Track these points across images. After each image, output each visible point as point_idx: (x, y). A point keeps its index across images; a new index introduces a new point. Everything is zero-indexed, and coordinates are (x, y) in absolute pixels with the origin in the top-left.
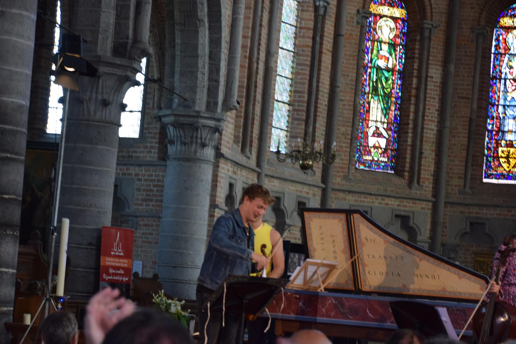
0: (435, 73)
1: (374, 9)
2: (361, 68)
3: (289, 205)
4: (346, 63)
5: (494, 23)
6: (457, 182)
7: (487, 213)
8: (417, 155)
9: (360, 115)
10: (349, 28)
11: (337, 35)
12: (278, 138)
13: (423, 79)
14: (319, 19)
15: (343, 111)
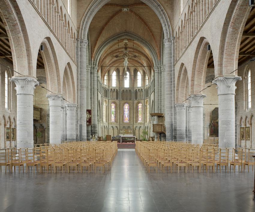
0: (118, 111)
1: (112, 105)
2: (111, 111)
3: (106, 126)
4: (109, 111)
5: (124, 105)
6: (122, 122)
7: (125, 125)
8: (117, 120)
9: (111, 116)
10: (109, 107)
11: (108, 108)
12: (104, 120)
13: (117, 112)
14: (106, 107)
15: (110, 116)
